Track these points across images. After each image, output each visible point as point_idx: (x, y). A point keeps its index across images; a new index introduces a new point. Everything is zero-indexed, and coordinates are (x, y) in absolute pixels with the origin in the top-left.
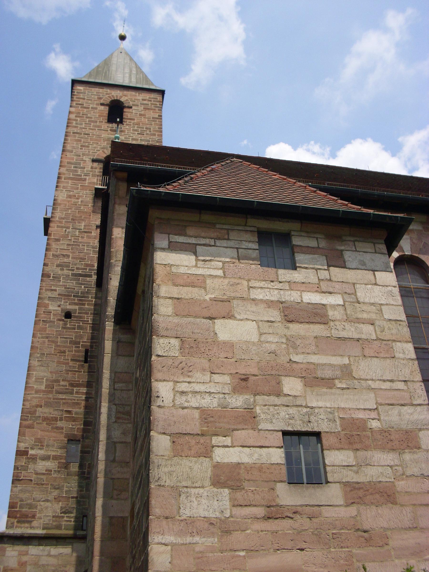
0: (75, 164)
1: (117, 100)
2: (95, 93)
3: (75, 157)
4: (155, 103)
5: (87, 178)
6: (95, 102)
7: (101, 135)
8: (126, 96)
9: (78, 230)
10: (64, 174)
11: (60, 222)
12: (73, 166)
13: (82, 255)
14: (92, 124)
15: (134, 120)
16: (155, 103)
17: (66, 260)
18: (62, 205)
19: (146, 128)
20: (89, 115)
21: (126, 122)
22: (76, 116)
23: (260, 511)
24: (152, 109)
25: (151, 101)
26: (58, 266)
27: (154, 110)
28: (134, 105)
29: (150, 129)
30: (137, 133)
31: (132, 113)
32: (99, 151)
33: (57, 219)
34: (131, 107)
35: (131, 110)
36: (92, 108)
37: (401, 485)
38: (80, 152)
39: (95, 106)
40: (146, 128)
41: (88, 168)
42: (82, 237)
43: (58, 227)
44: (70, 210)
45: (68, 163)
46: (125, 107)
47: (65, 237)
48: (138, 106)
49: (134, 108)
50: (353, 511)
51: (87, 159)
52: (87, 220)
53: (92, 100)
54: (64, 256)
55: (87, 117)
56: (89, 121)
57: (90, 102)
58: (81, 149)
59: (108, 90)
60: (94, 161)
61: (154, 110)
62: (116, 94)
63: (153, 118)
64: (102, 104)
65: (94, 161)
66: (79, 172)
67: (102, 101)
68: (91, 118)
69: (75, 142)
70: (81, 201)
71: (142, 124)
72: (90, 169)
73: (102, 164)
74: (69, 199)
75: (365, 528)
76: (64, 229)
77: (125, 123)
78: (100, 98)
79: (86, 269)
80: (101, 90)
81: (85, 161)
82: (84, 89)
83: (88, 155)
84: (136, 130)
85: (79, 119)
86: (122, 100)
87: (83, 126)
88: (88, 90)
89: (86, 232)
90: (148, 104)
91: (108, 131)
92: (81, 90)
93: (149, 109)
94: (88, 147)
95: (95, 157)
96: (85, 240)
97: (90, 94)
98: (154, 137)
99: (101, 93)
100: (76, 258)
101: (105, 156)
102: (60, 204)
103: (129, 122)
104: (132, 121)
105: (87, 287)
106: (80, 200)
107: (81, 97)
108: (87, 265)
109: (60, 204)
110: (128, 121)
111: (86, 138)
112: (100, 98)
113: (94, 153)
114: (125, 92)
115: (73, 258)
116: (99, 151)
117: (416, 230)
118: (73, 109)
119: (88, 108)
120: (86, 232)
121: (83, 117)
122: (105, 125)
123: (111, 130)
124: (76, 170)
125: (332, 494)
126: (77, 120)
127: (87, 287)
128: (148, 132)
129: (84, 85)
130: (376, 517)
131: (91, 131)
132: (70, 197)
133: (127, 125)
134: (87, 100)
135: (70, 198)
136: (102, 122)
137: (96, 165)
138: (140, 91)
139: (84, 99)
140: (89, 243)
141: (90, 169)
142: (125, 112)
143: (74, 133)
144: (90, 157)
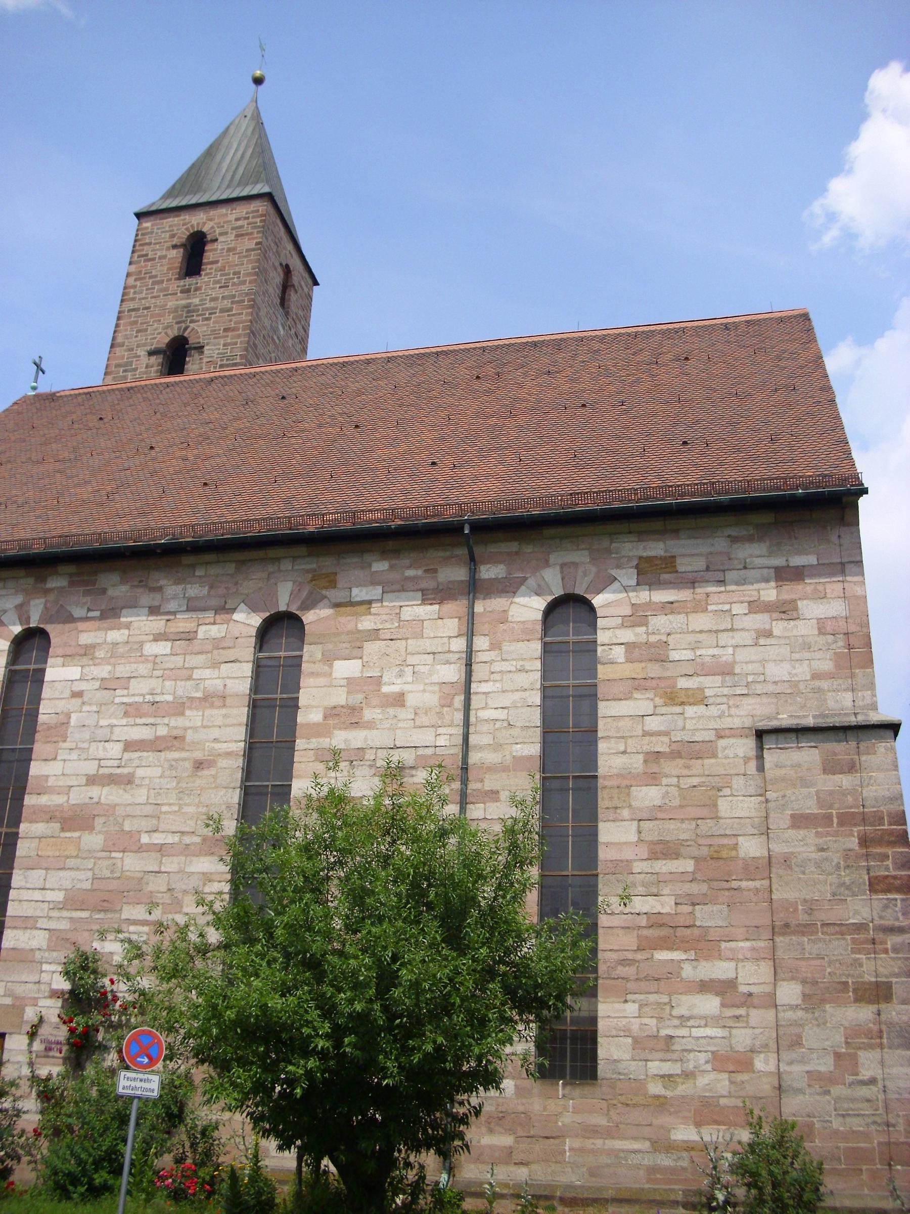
0: (126, 364)
1: (198, 231)
8: (211, 220)
12: (122, 369)
14: (156, 287)
21: (207, 269)
22: (136, 280)
27: (252, 233)
28: (221, 234)
29: (239, 273)
30: (218, 286)
32: (160, 333)
35: (215, 245)
36: (160, 258)
39: (164, 253)
41: (141, 368)
49: (221, 239)
51: (142, 352)
55: (150, 277)
59: (187, 217)
60: (151, 353)
63: (247, 250)
64: (175, 247)
65: (151, 353)
67: (176, 241)
68: (156, 276)
72: (144, 370)
78: (173, 236)
80: (176, 219)
81: (139, 356)
83: (144, 345)
84: (218, 282)
87: (143, 295)
88: (157, 225)
92: (147, 228)
93: (242, 235)
94: (146, 330)
98: (243, 287)
99: (175, 225)
101: (167, 340)
103: (211, 269)
104: (214, 266)
111: (144, 316)
116: (160, 333)
117: (58, 588)
118: (133, 268)
122: (175, 286)
123: (182, 292)
129: (152, 218)
131: (153, 301)
133: (206, 274)
138: (234, 205)
139: (150, 244)
141: (144, 370)
144: (146, 348)
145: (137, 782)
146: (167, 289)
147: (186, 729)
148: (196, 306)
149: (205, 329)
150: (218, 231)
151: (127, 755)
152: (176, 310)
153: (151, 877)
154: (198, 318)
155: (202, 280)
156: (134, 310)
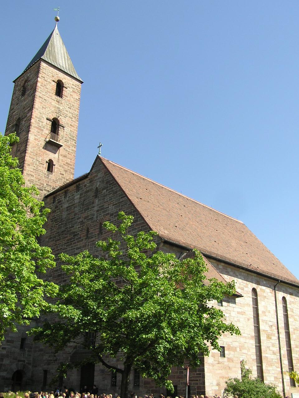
2: (51, 72)
3: (39, 114)
4: (78, 89)
5: (44, 129)
6: (51, 78)
7: (52, 103)
9: (38, 162)
10: (34, 124)
11: (31, 154)
13: (39, 177)
15: (67, 97)
16: (78, 89)
17: (32, 178)
18: (32, 144)
19: (72, 105)
20: (47, 87)
21: (64, 97)
23: (217, 362)
24: (76, 93)
25: (76, 87)
26: (29, 181)
31: (67, 92)
33: (29, 152)
34: (67, 88)
37: (234, 359)
38: (42, 111)
39: (50, 81)
40: (72, 105)
42: (40, 167)
43: (29, 157)
44: (35, 148)
45: (36, 117)
46: (63, 87)
47: (33, 164)
48: (70, 88)
50: (228, 363)
52: (42, 156)
53: (49, 76)
54: (32, 175)
55: (46, 88)
56: (47, 91)
57: (48, 77)
58: (42, 109)
61: (77, 93)
62: (61, 76)
66: (41, 124)
67: (54, 79)
69: (40, 104)
70: (41, 144)
71: (71, 101)
73: (51, 122)
74: (35, 141)
75: (229, 366)
76: (32, 159)
77: (63, 98)
79: (41, 186)
81: (43, 118)
82: (46, 66)
85: (42, 87)
86: (63, 81)
89: (41, 164)
90: (74, 89)
91: (55, 101)
94: (45, 109)
95: (48, 117)
96: (41, 168)
97: (49, 71)
100: (37, 178)
102: (31, 143)
105: (40, 196)
106: (40, 143)
107: (44, 72)
108: (41, 184)
109: (31, 143)
110: (65, 97)
112: (53, 76)
113: (48, 114)
114: (65, 76)
115: (35, 177)
119: (47, 81)
120: (41, 164)
121: (44, 87)
123: (57, 101)
124: (39, 123)
125: (225, 359)
126: (41, 88)
127: (40, 196)
128: (73, 108)
130: (231, 365)
132: (35, 139)
133: (64, 99)
134: (47, 75)
135: (36, 140)
136: (53, 94)
137: (48, 121)
140: (43, 171)
142: (64, 90)
143: (39, 97)
145: (240, 321)
146: (51, 96)
147: (246, 311)
148: (61, 109)
149: (64, 120)
150: (67, 85)
151: (238, 315)
152: (55, 107)
153: (245, 343)
154: (62, 115)
155: (62, 100)
156: (41, 97)
